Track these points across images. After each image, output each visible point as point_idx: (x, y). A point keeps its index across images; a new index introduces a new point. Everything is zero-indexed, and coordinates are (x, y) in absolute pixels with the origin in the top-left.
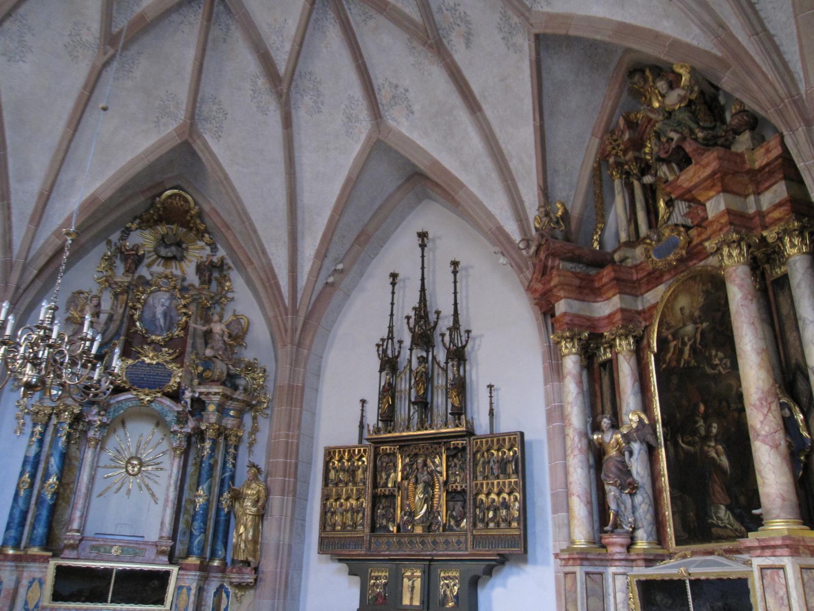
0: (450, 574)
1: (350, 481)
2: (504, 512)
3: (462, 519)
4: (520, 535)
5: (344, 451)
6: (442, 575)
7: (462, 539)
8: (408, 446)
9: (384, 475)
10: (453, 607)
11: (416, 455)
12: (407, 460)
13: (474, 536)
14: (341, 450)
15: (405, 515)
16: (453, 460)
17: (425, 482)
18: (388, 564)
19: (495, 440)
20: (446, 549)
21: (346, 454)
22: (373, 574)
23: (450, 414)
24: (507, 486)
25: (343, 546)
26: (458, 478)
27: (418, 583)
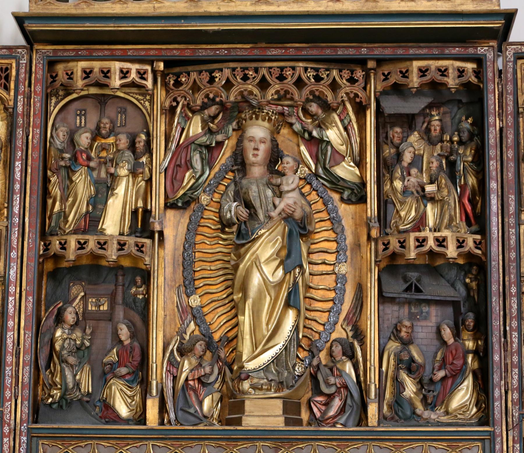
3: (456, 377)
9: (82, 185)
11: (236, 113)
12: (195, 127)
15: (183, 352)
16: (404, 139)
17: (287, 218)
26: (431, 212)
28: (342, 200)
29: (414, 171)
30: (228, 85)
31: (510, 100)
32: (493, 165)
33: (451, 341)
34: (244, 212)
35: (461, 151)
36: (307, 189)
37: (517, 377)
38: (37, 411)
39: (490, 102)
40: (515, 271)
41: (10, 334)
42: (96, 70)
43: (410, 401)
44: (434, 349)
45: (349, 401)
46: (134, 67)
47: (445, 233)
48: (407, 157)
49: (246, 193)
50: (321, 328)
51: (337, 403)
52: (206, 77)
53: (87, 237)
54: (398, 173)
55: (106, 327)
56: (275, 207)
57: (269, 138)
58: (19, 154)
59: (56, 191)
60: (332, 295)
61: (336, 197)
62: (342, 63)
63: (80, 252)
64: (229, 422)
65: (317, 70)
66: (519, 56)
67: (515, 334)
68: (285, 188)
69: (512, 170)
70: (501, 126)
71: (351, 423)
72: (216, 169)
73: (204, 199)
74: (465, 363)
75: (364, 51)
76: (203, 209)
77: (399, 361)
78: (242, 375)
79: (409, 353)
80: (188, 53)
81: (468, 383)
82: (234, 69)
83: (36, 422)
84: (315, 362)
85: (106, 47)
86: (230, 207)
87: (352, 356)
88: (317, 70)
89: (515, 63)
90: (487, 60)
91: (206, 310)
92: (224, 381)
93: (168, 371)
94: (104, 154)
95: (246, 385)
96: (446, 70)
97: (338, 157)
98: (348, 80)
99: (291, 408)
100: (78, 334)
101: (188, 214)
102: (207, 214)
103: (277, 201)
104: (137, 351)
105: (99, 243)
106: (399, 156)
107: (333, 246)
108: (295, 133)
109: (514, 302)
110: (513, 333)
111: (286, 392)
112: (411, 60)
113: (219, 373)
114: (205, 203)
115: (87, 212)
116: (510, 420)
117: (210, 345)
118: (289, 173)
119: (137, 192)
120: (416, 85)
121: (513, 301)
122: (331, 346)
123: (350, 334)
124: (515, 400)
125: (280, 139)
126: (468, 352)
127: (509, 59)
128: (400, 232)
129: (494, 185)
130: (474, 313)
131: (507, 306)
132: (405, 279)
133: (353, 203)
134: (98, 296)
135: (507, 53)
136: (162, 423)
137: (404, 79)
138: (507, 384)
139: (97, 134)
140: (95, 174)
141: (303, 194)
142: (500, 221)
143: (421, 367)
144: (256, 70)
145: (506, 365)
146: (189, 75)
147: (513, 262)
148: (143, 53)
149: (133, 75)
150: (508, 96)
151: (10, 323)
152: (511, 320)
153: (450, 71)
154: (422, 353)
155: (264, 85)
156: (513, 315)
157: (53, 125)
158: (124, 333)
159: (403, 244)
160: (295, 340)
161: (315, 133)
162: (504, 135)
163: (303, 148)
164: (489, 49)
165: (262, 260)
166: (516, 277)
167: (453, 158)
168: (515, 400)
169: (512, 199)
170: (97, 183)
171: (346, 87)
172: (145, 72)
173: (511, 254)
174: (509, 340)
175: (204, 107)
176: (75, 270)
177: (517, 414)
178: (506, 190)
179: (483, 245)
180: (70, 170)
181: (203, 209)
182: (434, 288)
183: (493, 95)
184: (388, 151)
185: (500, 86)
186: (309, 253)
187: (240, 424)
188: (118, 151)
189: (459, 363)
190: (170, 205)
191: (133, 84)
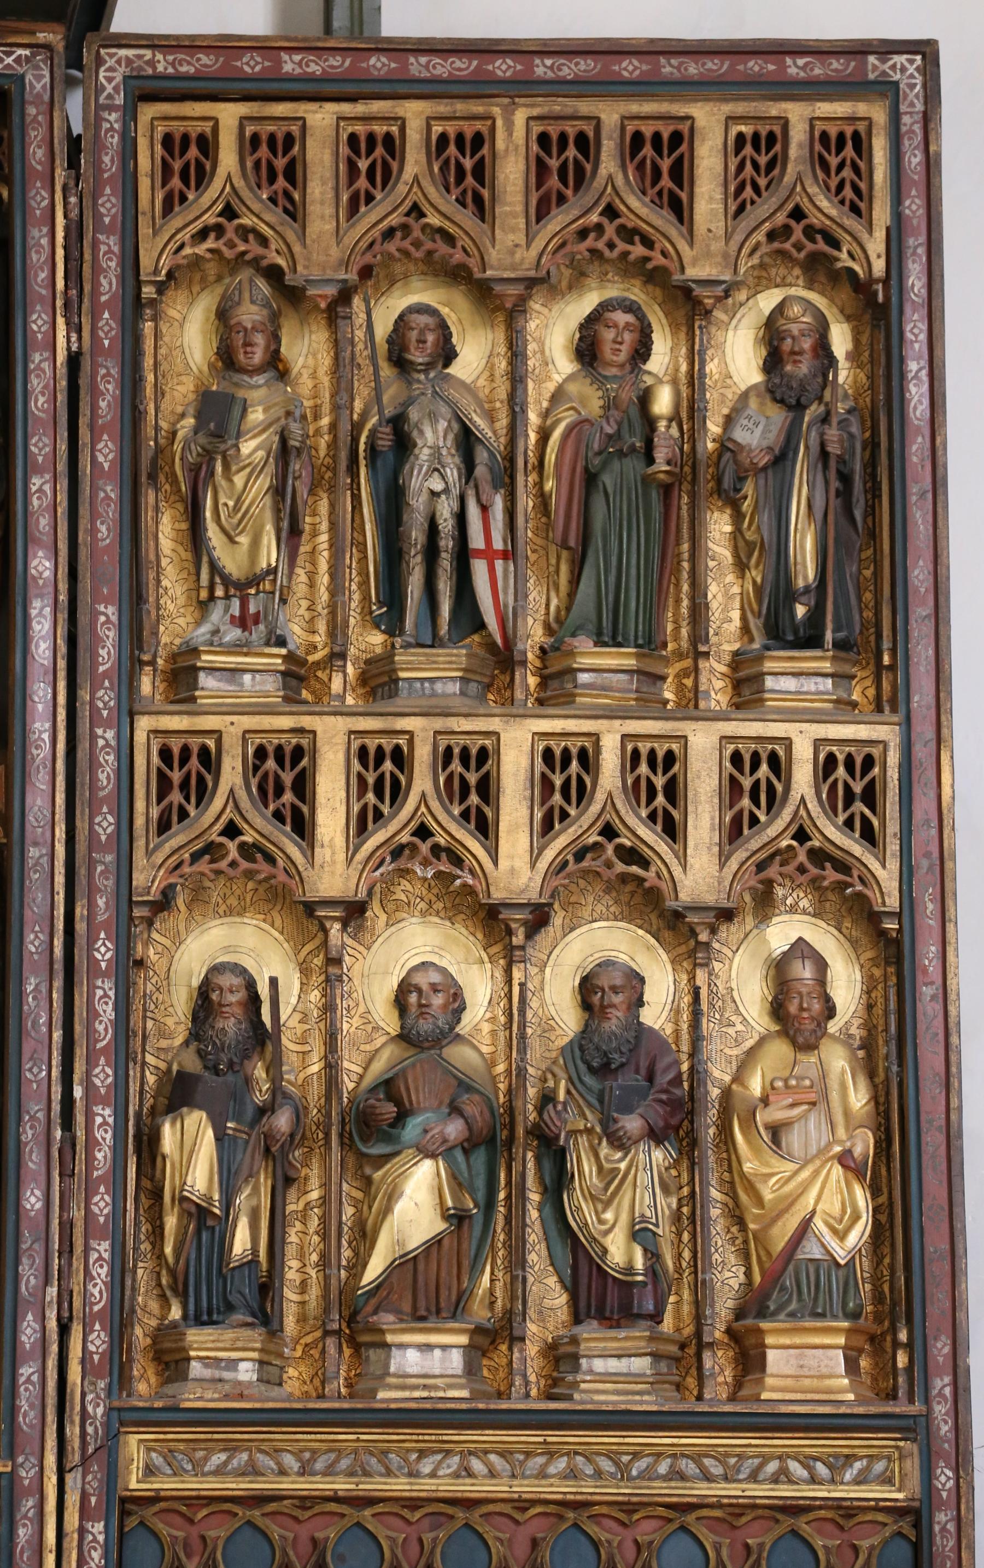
2: (624, 1201)
4: (915, 1517)
13: (125, 1508)
19: (513, 135)
31: (110, 251)
32: (40, 490)
37: (104, 1271)
39: (34, 257)
40: (110, 883)
66: (144, 90)
67: (104, 1114)
69: (112, 512)
70: (74, 347)
89: (130, 113)
90: (28, 97)
109: (106, 995)
110: (98, 1109)
116: (73, 1431)
121: (99, 993)
124: (96, 1357)
127: (110, 97)
129: (42, 566)
131: (76, 1010)
135: (102, 74)
138: (66, 1296)
142: (62, 699)
145: (67, 1227)
147: (104, 849)
150: (102, 237)
152: (91, 1062)
156: (99, 1046)
162: (83, 382)
164: (34, 55)
166: (112, 903)
168: (96, 1357)
169: (106, 618)
173: (97, 820)
174: (80, 1134)
177: (100, 1411)
178: (85, 582)
183: (45, 230)
185: (73, 200)
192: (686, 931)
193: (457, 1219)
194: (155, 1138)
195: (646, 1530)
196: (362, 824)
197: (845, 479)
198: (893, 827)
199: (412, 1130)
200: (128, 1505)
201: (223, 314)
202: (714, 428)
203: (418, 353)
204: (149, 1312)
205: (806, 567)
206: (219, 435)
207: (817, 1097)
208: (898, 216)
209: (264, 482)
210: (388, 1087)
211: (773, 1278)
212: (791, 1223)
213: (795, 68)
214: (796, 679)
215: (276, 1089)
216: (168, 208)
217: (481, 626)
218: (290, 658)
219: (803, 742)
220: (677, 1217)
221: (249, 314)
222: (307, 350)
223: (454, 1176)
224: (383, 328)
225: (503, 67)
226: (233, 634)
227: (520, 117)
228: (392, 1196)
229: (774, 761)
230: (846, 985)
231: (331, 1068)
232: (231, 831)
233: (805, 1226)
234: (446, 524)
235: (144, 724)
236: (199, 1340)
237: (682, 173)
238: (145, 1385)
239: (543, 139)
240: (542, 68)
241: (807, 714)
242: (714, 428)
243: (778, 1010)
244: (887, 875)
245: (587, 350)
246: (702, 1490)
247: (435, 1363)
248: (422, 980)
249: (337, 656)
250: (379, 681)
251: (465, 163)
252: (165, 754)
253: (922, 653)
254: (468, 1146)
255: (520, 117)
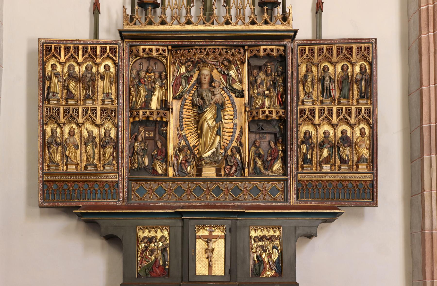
0: (265, 233)
1: (87, 96)
2: (346, 152)
3: (275, 159)
4: (373, 181)
5: (76, 49)
6: (253, 234)
7: (280, 186)
8: (188, 47)
10: (273, 276)
11: (198, 64)
12: (183, 70)
13: (298, 181)
14: (72, 48)
15: (180, 150)
16: (258, 75)
17: (216, 103)
18: (167, 221)
20: (255, 200)
21: (80, 52)
22: (141, 234)
23: (279, 4)
24: (353, 115)
25: (82, 195)
27: (219, 247)
28: (235, 96)
29: (261, 86)
30: (195, 54)
33: (274, 147)
34: (201, 102)
35: (278, 79)
36: (223, 92)
38: (131, 172)
41: (120, 145)
42: (147, 49)
43: (259, 168)
44: (267, 150)
45: (238, 168)
46: (161, 48)
47: (272, 109)
48: (259, 81)
49: (202, 94)
50: (228, 142)
51: (234, 168)
52: (186, 51)
53: (146, 110)
54: (255, 87)
55: (151, 142)
56: (212, 99)
57: (209, 74)
58: (121, 80)
59: (133, 93)
60: (232, 130)
61: (233, 95)
62: (235, 47)
63: (144, 116)
64: (197, 175)
65: (227, 49)
66: (299, 45)
67: (296, 145)
68: (216, 93)
71: (239, 175)
72: (190, 85)
73: (186, 96)
74: (278, 154)
75: (244, 43)
76: (186, 99)
77: (255, 153)
78: (200, 159)
79: (259, 151)
80: (180, 43)
81: (279, 161)
82: (197, 49)
83: (130, 175)
84: (226, 154)
85: (151, 41)
86: (196, 99)
87: (239, 152)
88: (227, 49)
89: (297, 47)
91: (187, 136)
92: (194, 160)
93: (175, 158)
94: (150, 79)
95: (203, 162)
96: (273, 49)
97: (234, 81)
98: (238, 53)
99: (218, 171)
100: (142, 145)
101: (180, 101)
102: (187, 101)
103: (213, 97)
104: (164, 150)
105: (150, 113)
106: (256, 80)
107: (232, 113)
108: (218, 71)
111: (216, 165)
112: (260, 46)
113: (193, 158)
114: (186, 97)
115: (145, 101)
117: (189, 148)
118: (217, 87)
119: (163, 93)
120: (262, 55)
122: (232, 149)
123: (238, 144)
125: (213, 74)
126: (279, 151)
128: (256, 108)
129: (289, 92)
130: (282, 137)
132: (258, 125)
133: (239, 97)
134: (149, 131)
136: (173, 176)
137: (258, 53)
139: (147, 71)
140: (147, 87)
141: (222, 95)
143: (263, 156)
144: (205, 49)
145: (292, 155)
146: (180, 50)
148: (164, 43)
149: (161, 51)
151: (120, 141)
153: (274, 50)
154: (263, 151)
155: (207, 54)
157: (131, 69)
158: (159, 144)
159: (257, 113)
160: (219, 147)
161: (226, 72)
163: (221, 77)
165: (208, 118)
167: (275, 81)
170: (148, 90)
171: (237, 56)
172: (165, 50)
175: (186, 62)
176: (141, 122)
179: (285, 113)
180: (138, 86)
181: (186, 99)
182: (267, 128)
184: (252, 79)
186: (224, 115)
187: (201, 176)
188: (155, 78)
189: (276, 154)
190: (174, 98)
191: (160, 54)
192: (351, 126)
193: (329, 154)
194: (300, 147)
195: (347, 183)
196: (320, 117)
197: (368, 81)
198: (372, 116)
199: (325, 146)
200: (299, 181)
201: (306, 66)
202: (355, 76)
203: (326, 69)
204: (300, 163)
205: (364, 91)
206: (306, 79)
207: (364, 142)
208: (373, 55)
209: (310, 83)
210: (323, 142)
211: (359, 159)
212: (361, 154)
213: (363, 41)
214: (362, 101)
215: (312, 142)
216: (301, 57)
217: (331, 97)
218: (313, 100)
219: (363, 108)
220: (350, 154)
221: (309, 67)
222: (314, 69)
223: (329, 151)
224: (322, 68)
225: (334, 42)
226: (307, 98)
227: (335, 46)
228: (323, 152)
229: (360, 110)
230: (367, 131)
231: (317, 140)
232: (307, 117)
233: (363, 154)
234: (328, 87)
235: (299, 107)
236: (305, 166)
237: (352, 51)
238: (300, 169)
239: (338, 48)
240: (338, 42)
241: (364, 105)
242: (355, 76)
243: (360, 134)
244: (371, 121)
245: (342, 69)
246: (352, 179)
247: (327, 168)
248: (326, 132)
249: (317, 100)
250: (322, 102)
251: (330, 51)
252: (301, 110)
253: (375, 99)
254: (330, 147)
255: (335, 46)
